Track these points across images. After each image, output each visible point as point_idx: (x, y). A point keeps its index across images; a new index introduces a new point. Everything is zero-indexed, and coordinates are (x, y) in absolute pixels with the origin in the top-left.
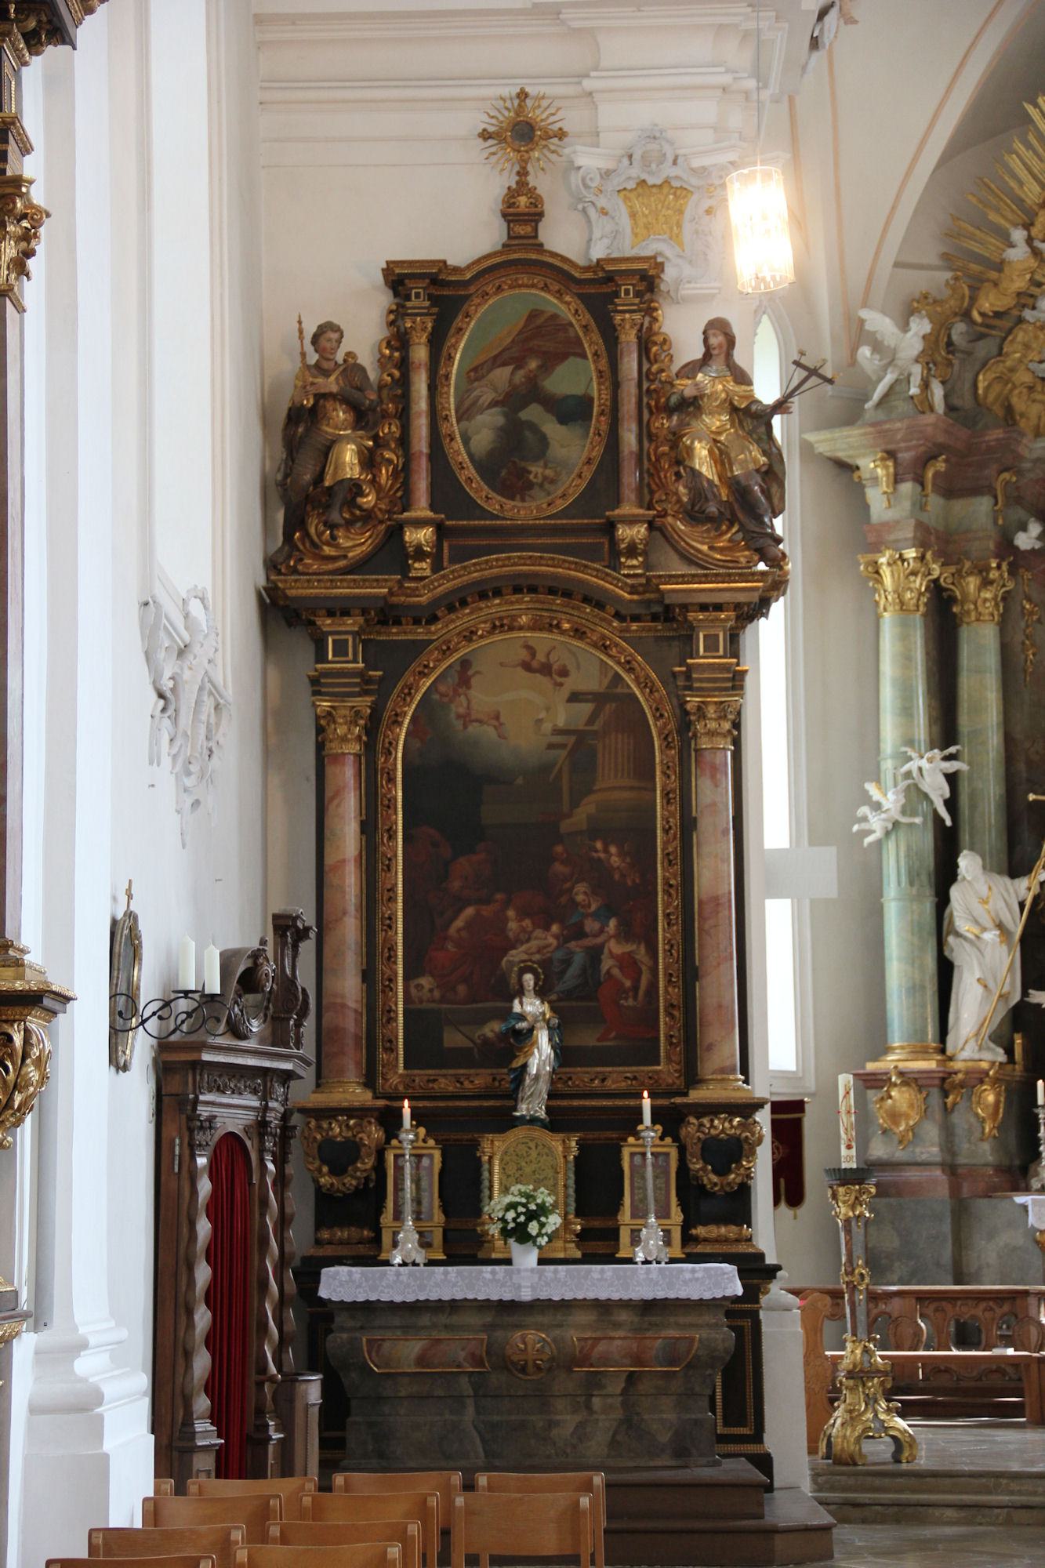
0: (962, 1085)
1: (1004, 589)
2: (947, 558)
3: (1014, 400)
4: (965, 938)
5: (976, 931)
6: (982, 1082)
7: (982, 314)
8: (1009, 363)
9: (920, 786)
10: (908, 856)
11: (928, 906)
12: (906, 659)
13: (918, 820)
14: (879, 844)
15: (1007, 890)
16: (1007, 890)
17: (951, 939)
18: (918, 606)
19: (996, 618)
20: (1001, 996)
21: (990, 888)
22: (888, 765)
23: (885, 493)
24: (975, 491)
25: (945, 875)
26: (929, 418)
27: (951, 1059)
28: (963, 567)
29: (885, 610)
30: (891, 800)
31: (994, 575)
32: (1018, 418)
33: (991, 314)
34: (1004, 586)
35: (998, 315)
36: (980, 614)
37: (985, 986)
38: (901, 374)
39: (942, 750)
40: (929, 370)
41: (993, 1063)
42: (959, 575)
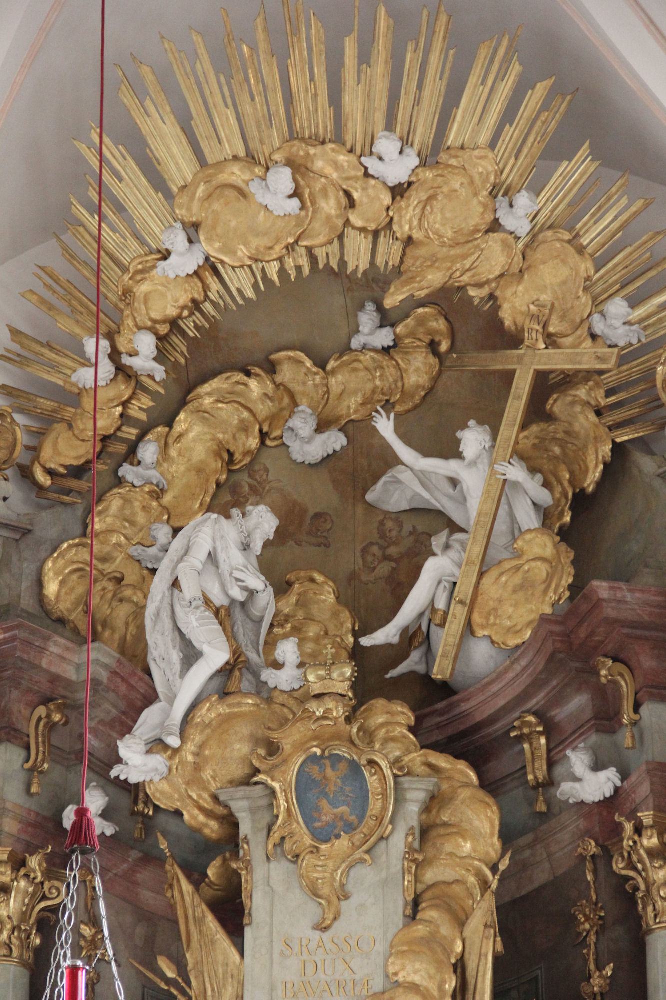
1: (43, 905)
7: (50, 473)
19: (16, 953)
33: (62, 471)
34: (44, 898)
35: (78, 472)
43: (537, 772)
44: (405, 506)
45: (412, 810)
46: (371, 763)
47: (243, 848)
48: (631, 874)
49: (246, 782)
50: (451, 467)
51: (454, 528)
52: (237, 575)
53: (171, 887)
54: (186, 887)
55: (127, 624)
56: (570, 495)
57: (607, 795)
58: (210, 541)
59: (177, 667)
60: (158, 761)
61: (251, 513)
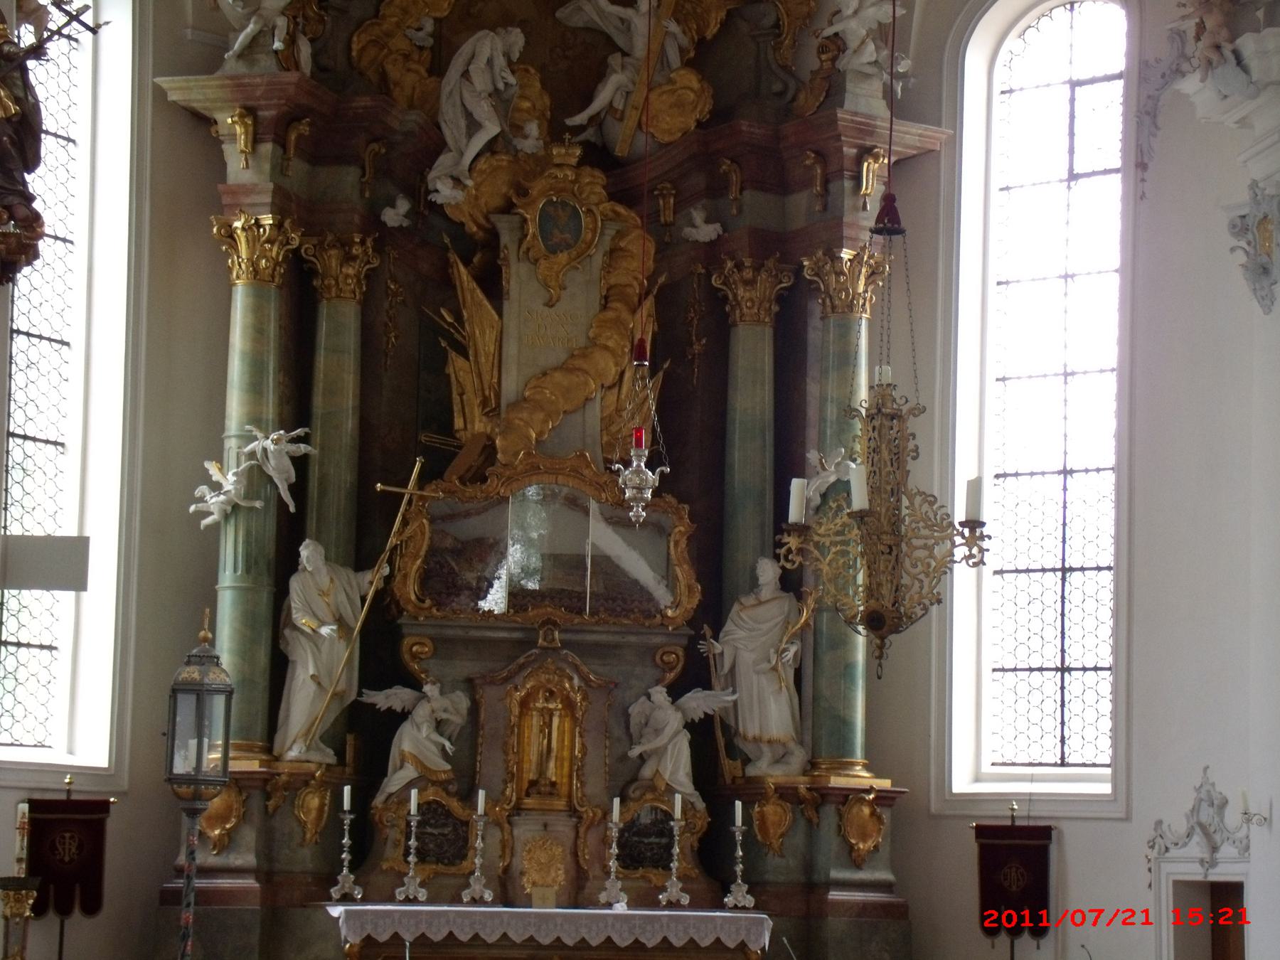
0: (287, 786)
1: (368, 267)
2: (310, 228)
3: (389, 67)
4: (303, 632)
5: (314, 624)
6: (307, 784)
8: (385, 27)
9: (265, 469)
10: (247, 542)
11: (265, 597)
12: (257, 332)
13: (258, 504)
14: (215, 527)
15: (350, 583)
16: (350, 583)
17: (287, 632)
18: (273, 277)
19: (358, 297)
20: (335, 695)
21: (332, 580)
22: (231, 444)
23: (242, 152)
24: (341, 159)
25: (286, 564)
26: (292, 77)
27: (277, 759)
28: (325, 240)
29: (238, 277)
30: (229, 482)
31: (357, 250)
32: (392, 86)
34: (369, 262)
36: (341, 290)
37: (319, 684)
38: (265, 25)
39: (287, 431)
40: (297, 24)
41: (320, 765)
42: (320, 247)
43: (667, 216)
44: (581, 24)
45: (607, 243)
46: (589, 211)
47: (503, 252)
48: (724, 288)
49: (508, 208)
50: (628, 13)
51: (625, 54)
52: (504, 74)
53: (452, 267)
54: (462, 268)
55: (414, 88)
56: (696, 38)
57: (713, 238)
58: (489, 50)
59: (464, 130)
60: (459, 195)
61: (511, 32)
